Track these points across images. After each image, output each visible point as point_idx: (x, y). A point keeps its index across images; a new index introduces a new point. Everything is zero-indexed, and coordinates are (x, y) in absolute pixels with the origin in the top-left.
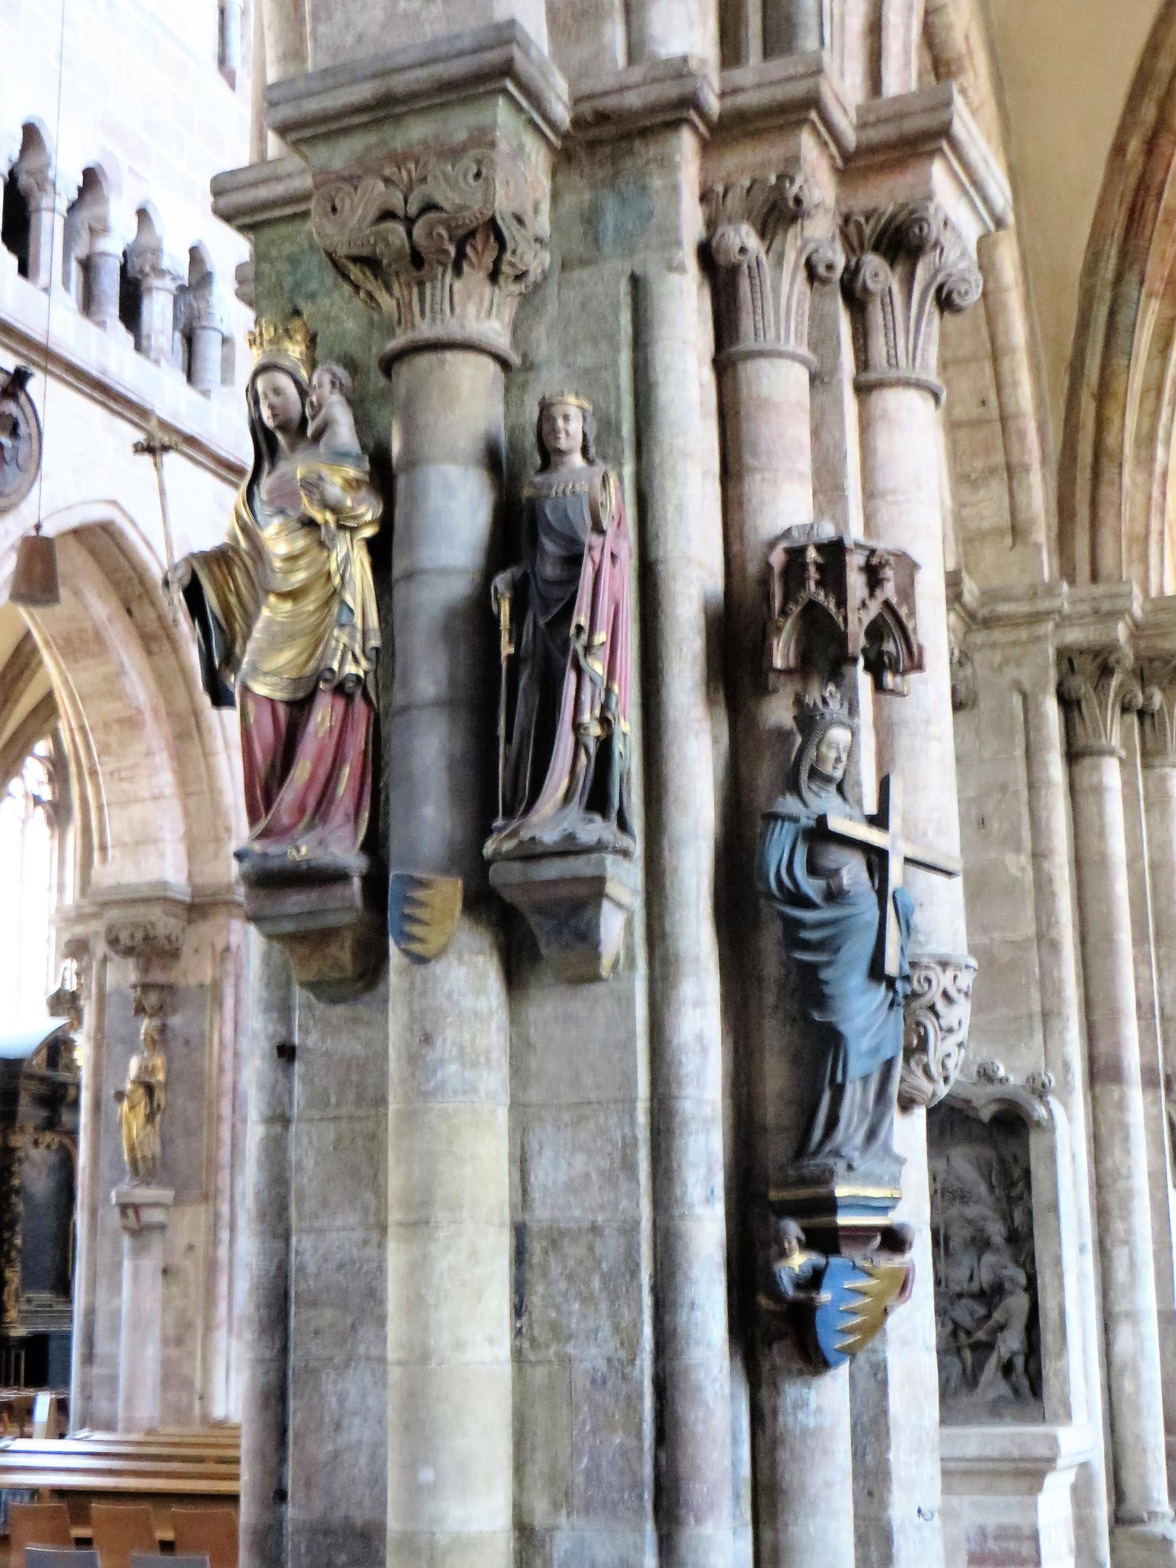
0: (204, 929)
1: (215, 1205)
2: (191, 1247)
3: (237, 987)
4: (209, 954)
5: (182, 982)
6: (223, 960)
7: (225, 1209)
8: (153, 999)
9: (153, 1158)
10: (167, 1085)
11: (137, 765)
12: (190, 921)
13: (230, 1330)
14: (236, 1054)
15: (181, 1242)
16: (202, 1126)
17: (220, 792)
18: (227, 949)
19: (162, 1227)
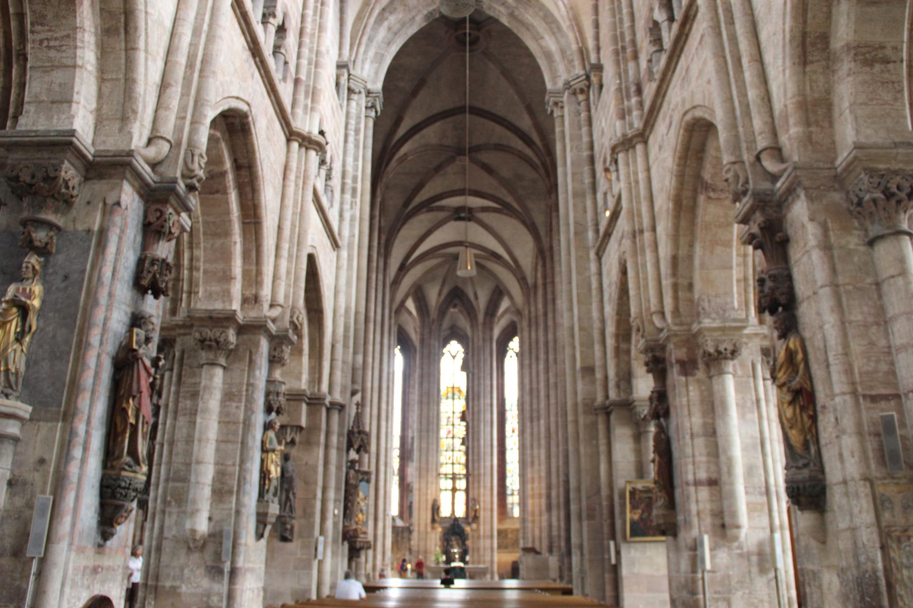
0: (98, 186)
1: (72, 422)
2: (42, 461)
3: (120, 238)
4: (101, 205)
5: (70, 227)
6: (112, 212)
7: (81, 428)
8: (40, 236)
9: (17, 373)
10: (41, 313)
11: (68, 36)
12: (87, 179)
13: (71, 544)
14: (111, 295)
15: (33, 453)
16: (69, 353)
17: (134, 81)
18: (118, 204)
19: (16, 440)
